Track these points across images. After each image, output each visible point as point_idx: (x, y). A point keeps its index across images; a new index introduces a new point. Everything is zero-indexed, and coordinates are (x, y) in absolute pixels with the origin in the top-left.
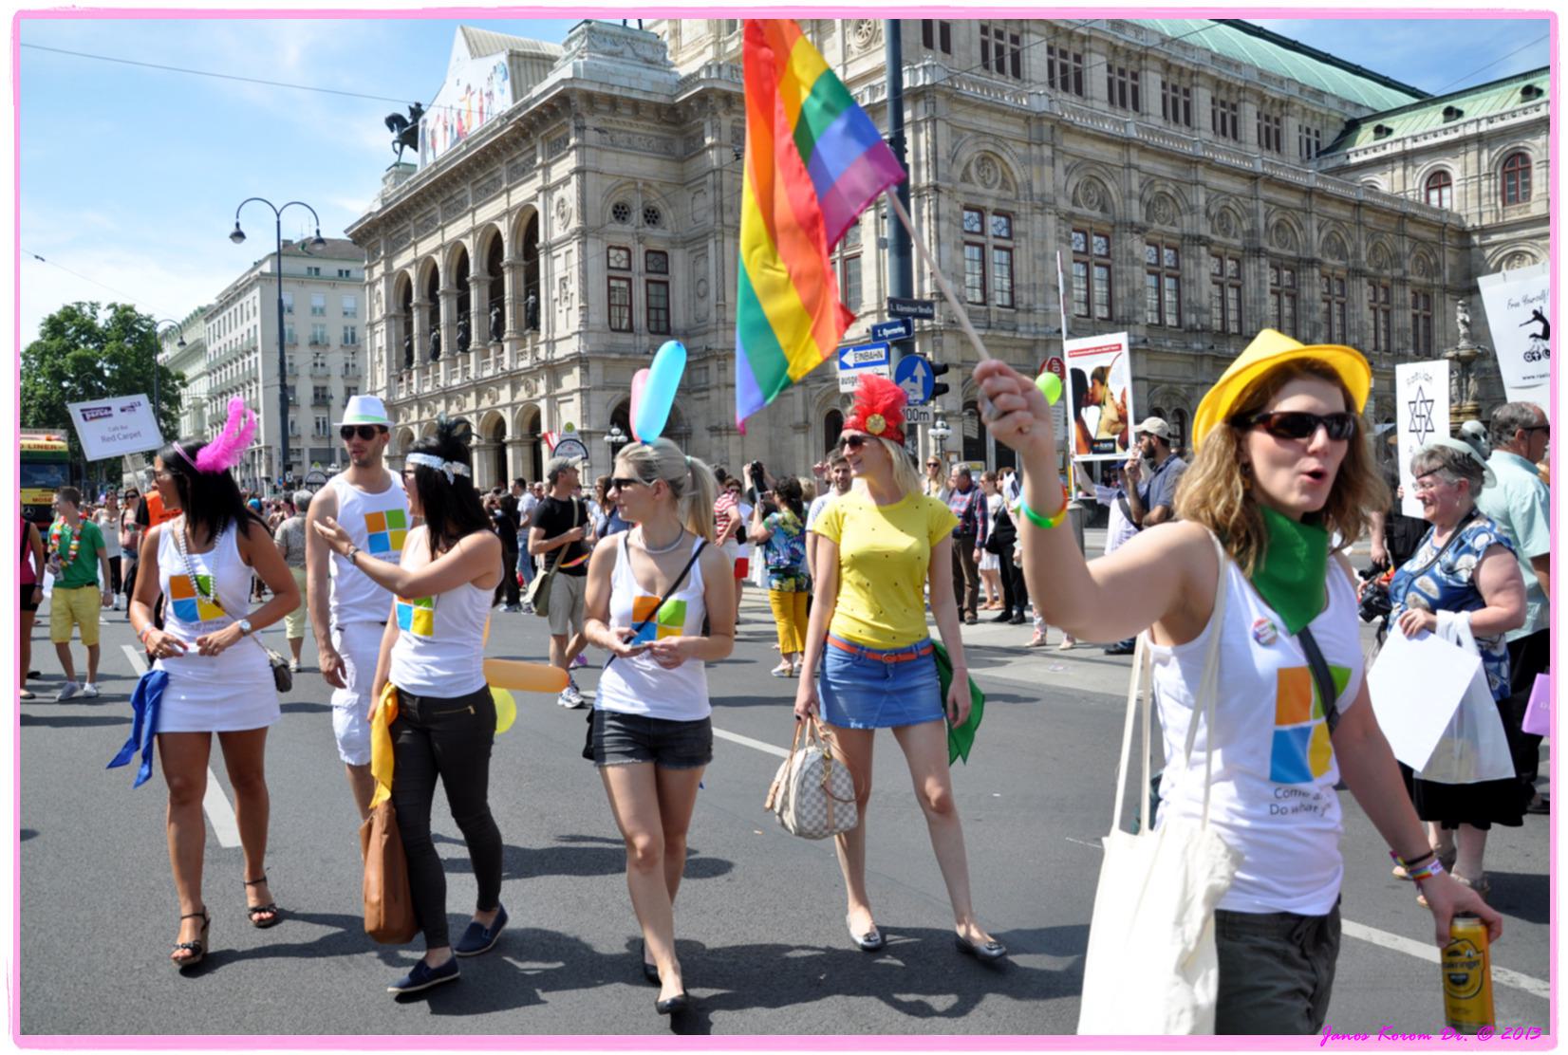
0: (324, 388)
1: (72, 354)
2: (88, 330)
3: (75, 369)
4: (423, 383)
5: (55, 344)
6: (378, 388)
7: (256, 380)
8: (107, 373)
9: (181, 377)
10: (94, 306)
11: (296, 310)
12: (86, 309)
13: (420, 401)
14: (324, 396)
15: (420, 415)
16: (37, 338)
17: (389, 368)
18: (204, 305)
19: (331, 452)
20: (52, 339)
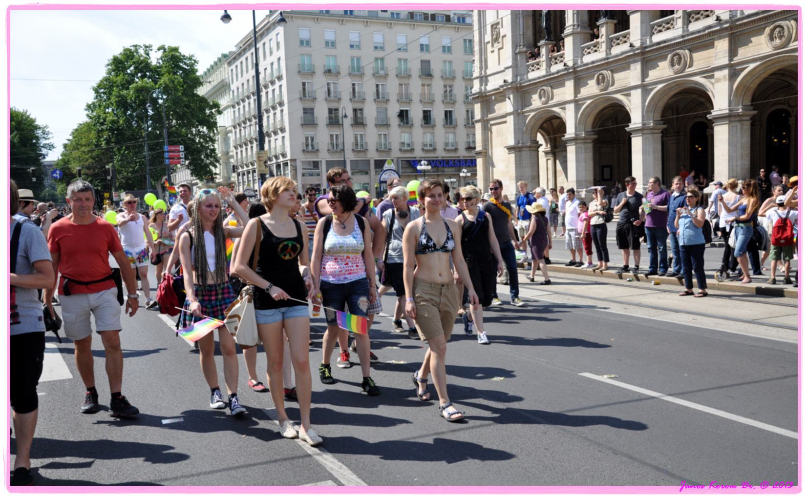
0: (337, 110)
1: (134, 85)
2: (144, 67)
3: (137, 97)
4: (579, 52)
5: (119, 79)
6: (489, 72)
7: (281, 104)
8: (160, 101)
9: (216, 106)
10: (147, 48)
11: (313, 43)
12: (141, 51)
13: (579, 75)
14: (337, 117)
15: (577, 91)
16: (105, 75)
17: (515, 45)
18: (226, 52)
19: (345, 161)
20: (117, 76)
